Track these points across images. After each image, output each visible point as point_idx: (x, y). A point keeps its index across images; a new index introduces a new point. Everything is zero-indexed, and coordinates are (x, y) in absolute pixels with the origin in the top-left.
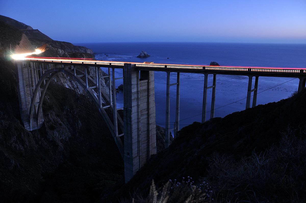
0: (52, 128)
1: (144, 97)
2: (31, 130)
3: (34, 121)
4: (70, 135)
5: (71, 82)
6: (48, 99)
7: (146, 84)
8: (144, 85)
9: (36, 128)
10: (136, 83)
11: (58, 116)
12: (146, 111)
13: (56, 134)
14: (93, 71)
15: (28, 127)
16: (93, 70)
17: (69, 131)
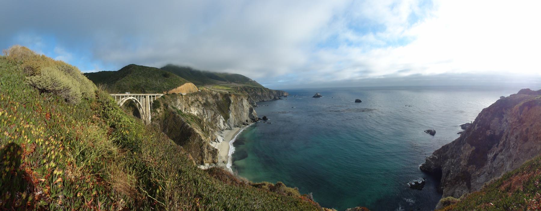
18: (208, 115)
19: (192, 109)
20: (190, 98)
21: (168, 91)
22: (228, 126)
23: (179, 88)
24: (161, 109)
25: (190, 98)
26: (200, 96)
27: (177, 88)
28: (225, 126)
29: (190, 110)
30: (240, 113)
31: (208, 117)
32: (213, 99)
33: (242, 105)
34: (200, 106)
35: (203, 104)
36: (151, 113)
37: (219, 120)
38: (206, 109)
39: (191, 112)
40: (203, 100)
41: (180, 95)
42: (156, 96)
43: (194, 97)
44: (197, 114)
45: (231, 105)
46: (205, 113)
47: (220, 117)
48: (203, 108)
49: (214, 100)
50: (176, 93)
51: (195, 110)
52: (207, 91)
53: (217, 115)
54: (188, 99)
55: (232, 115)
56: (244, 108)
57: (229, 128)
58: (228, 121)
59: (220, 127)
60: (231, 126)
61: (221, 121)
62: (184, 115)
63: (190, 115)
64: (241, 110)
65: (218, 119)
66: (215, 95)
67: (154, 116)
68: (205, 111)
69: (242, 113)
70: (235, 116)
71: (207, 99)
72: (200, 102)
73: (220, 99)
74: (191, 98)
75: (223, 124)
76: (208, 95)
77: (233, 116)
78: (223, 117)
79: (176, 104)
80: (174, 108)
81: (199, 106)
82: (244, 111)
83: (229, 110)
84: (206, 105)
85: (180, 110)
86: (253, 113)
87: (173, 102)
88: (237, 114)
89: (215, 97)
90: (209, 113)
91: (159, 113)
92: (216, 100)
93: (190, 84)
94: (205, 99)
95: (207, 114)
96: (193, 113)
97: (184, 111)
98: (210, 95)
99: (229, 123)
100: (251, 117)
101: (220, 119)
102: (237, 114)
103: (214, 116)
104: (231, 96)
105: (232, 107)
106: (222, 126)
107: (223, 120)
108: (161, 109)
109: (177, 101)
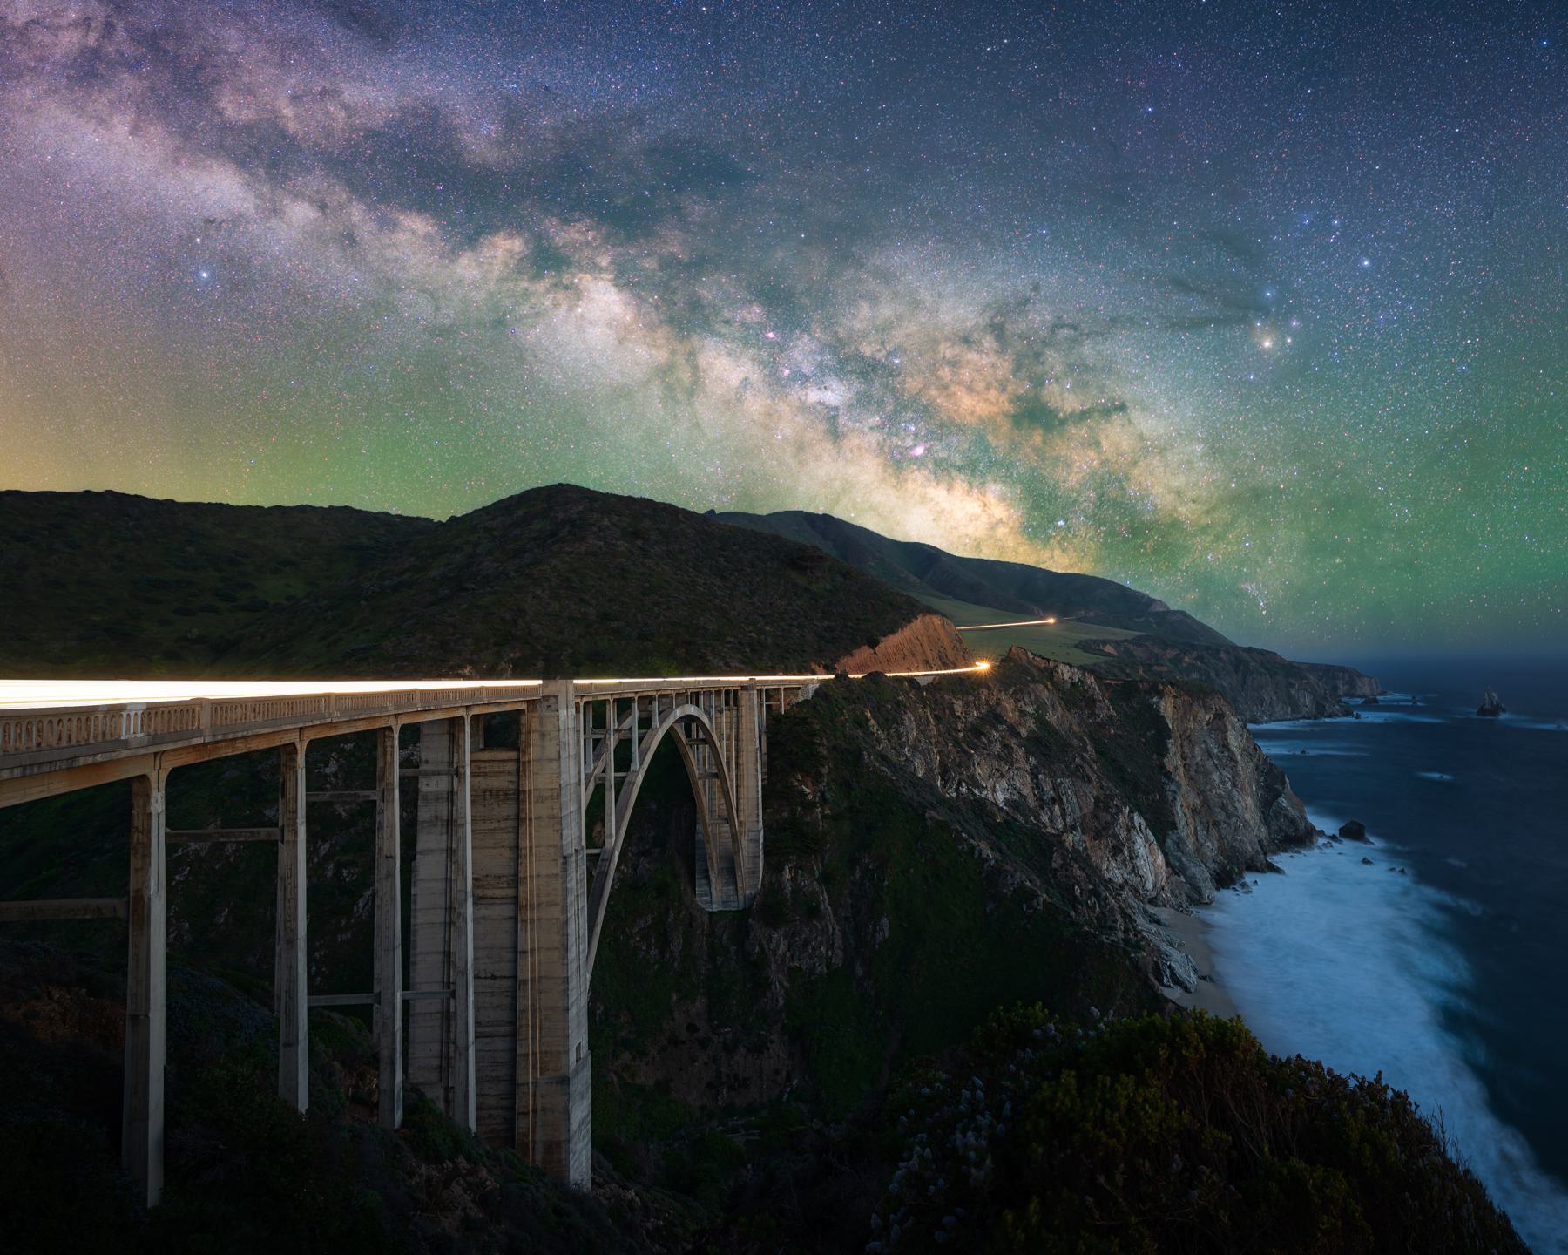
1: (499, 821)
5: (1034, 776)
6: (824, 817)
7: (511, 766)
8: (496, 769)
12: (505, 886)
14: (1201, 749)
24: (817, 778)
25: (958, 706)
26: (1006, 691)
30: (1220, 796)
32: (1069, 711)
33: (1225, 746)
34: (1020, 752)
35: (1028, 738)
36: (764, 809)
37: (1129, 839)
39: (976, 791)
43: (979, 699)
44: (1007, 802)
47: (1132, 819)
48: (1033, 761)
52: (1029, 662)
55: (1182, 806)
58: (1169, 842)
60: (1193, 877)
64: (1223, 782)
65: (1123, 834)
68: (1048, 787)
69: (1229, 793)
70: (1194, 811)
71: (1041, 706)
72: (1014, 732)
73: (1105, 709)
74: (967, 705)
76: (1041, 687)
77: (1186, 811)
78: (1143, 822)
82: (1239, 783)
83: (1168, 775)
88: (1205, 802)
89: (1074, 697)
90: (1069, 794)
93: (937, 620)
97: (939, 783)
99: (1180, 861)
101: (1133, 833)
102: (1205, 802)
103: (1095, 817)
104: (1161, 694)
105: (1173, 761)
109: (902, 719)
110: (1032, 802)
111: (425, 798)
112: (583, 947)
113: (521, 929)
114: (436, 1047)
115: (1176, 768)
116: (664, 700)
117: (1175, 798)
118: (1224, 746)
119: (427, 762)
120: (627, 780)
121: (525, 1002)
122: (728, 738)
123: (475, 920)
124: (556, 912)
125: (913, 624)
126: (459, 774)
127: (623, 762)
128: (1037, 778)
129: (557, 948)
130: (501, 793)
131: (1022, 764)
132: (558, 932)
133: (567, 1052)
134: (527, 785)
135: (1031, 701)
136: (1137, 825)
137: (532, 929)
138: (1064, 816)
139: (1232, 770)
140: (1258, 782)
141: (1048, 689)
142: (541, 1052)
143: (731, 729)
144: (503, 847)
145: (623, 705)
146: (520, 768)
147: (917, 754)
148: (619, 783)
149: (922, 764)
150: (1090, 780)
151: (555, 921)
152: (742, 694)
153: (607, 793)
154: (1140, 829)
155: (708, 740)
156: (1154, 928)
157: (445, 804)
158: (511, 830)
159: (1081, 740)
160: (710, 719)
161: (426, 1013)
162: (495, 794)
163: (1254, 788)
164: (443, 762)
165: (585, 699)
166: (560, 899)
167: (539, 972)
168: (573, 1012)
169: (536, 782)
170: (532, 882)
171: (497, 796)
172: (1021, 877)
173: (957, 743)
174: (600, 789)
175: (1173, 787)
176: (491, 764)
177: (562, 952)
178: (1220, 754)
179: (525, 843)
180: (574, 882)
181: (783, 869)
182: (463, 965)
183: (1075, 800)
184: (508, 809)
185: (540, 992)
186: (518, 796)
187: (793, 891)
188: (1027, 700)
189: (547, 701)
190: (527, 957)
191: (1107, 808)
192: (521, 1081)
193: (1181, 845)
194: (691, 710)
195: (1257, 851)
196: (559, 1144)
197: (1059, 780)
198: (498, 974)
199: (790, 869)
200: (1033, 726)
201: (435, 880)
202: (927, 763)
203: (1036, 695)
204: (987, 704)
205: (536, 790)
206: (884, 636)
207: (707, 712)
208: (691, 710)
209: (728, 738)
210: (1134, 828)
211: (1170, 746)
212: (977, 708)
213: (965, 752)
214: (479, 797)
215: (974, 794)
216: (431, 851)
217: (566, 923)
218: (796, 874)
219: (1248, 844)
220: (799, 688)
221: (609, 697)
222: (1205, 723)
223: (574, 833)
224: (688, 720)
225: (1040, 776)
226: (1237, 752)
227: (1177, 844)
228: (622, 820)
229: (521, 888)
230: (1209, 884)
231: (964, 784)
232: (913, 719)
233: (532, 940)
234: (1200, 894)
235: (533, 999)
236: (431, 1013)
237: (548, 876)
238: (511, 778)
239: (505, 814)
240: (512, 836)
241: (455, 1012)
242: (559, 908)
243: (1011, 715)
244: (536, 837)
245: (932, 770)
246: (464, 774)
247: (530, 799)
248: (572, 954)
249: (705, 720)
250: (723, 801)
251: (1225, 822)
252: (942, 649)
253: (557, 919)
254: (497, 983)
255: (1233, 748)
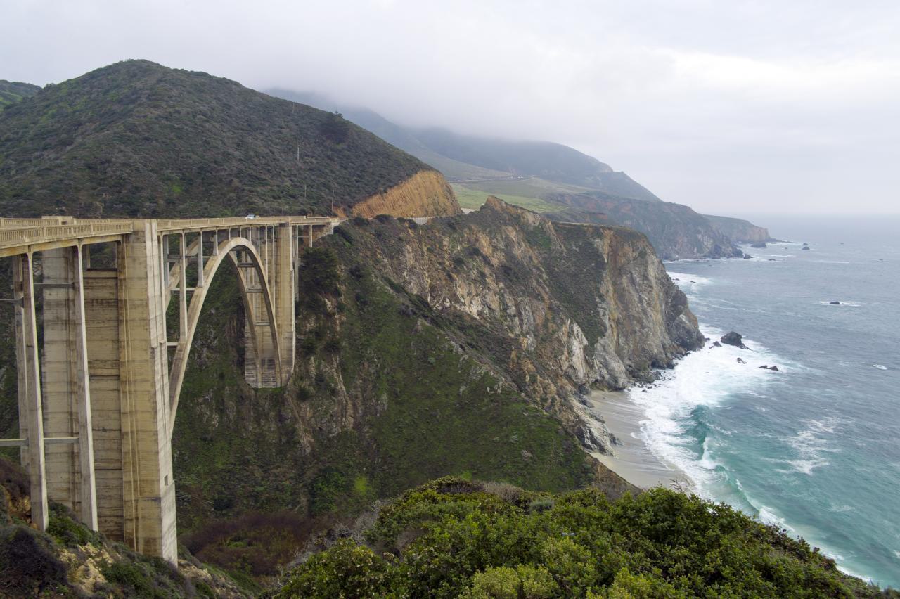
0: (303, 396)
1: (104, 322)
2: (260, 386)
3: (269, 365)
4: (351, 425)
6: (342, 323)
8: (100, 284)
9: (272, 385)
10: (63, 275)
11: (343, 369)
12: (110, 367)
13: (307, 410)
15: (253, 377)
16: (629, 275)
17: (353, 415)
18: (521, 320)
19: (460, 292)
20: (448, 239)
21: (350, 207)
22: (604, 372)
23: (395, 193)
27: (385, 192)
28: (592, 367)
29: (455, 295)
31: (525, 327)
32: (531, 248)
33: (645, 277)
35: (498, 269)
36: (296, 315)
37: (568, 342)
38: (512, 293)
39: (458, 306)
40: (495, 248)
41: (407, 225)
42: (314, 226)
44: (480, 314)
45: (606, 274)
46: (512, 310)
47: (571, 328)
48: (501, 285)
49: (533, 253)
50: (395, 214)
51: (469, 294)
53: (559, 321)
54: (441, 243)
55: (609, 319)
56: (654, 293)
57: (607, 377)
58: (598, 346)
59: (570, 371)
61: (577, 347)
62: (437, 321)
63: (461, 323)
65: (564, 339)
66: (536, 228)
67: (311, 332)
69: (644, 311)
70: (618, 322)
71: (509, 244)
72: (486, 261)
73: (559, 246)
74: (453, 240)
75: (586, 360)
76: (510, 228)
77: (612, 324)
78: (579, 330)
79: (398, 269)
80: (399, 289)
81: (483, 275)
84: (511, 273)
85: (417, 296)
86: (683, 317)
87: (386, 260)
89: (534, 236)
91: (334, 314)
92: (540, 254)
93: (432, 176)
94: (501, 246)
95: (519, 314)
96: (467, 309)
97: (429, 300)
98: (517, 231)
99: (605, 359)
100: (675, 332)
103: (545, 326)
105: (607, 287)
106: (582, 370)
107: (581, 343)
108: (337, 293)
109: (403, 253)
110: (498, 314)
111: (49, 304)
112: (167, 410)
113: (123, 397)
114: (65, 476)
115: (608, 291)
116: (222, 234)
117: (604, 315)
118: (644, 276)
119: (49, 278)
120: (195, 294)
121: (127, 447)
122: (270, 263)
123: (91, 391)
124: (147, 386)
125: (413, 178)
126: (74, 287)
127: (193, 281)
128: (503, 296)
129: (149, 411)
130: (104, 302)
131: (492, 285)
132: (149, 400)
133: (158, 481)
134: (124, 296)
135: (502, 239)
136: (575, 332)
137: (130, 398)
138: (521, 325)
139: (648, 293)
140: (667, 303)
141: (515, 228)
142: (140, 480)
143: (272, 256)
144: (107, 340)
145: (192, 237)
146: (118, 283)
147: (414, 277)
148: (190, 295)
149: (416, 284)
150: (543, 300)
151: (147, 393)
152: (280, 230)
153: (181, 303)
154: (577, 334)
155: (255, 264)
156: (581, 406)
157: (64, 308)
158: (113, 328)
159: (538, 269)
160: (256, 248)
161: (57, 453)
162: (102, 302)
163: (664, 307)
164: (60, 278)
165: (164, 233)
166: (150, 378)
167: (137, 427)
168: (161, 455)
169: (130, 294)
170: (128, 365)
171: (102, 303)
172: (484, 367)
173: (444, 270)
174: (175, 296)
175: (604, 306)
176: (96, 280)
177: (153, 413)
178: (641, 282)
179: (123, 337)
180: (160, 366)
181: (309, 359)
182: (84, 421)
183: (531, 314)
184: (111, 314)
185: (138, 441)
186: (117, 304)
187: (316, 376)
188: (499, 238)
189: (137, 234)
190: (127, 417)
191: (554, 320)
192: (126, 499)
193: (606, 348)
194: (242, 241)
195: (661, 352)
196: (155, 540)
197: (520, 299)
198: (106, 428)
199: (315, 359)
200: (503, 258)
201: (59, 362)
202: (420, 284)
203: (506, 234)
204: (469, 241)
205: (129, 300)
206: (391, 187)
207: (254, 243)
208: (242, 241)
209: (270, 263)
210: (573, 334)
211: (604, 275)
212: (461, 243)
213: (450, 276)
214: (89, 303)
215: (455, 308)
216: (53, 342)
217: (155, 394)
218: (320, 363)
219: (654, 347)
220: (324, 226)
221: (181, 232)
222: (631, 259)
223: (158, 332)
224: (240, 250)
225: (505, 295)
226: (653, 281)
227: (604, 347)
228: (193, 321)
229: (122, 369)
230: (624, 376)
231: (448, 300)
232: (411, 250)
233: (131, 405)
234: (616, 381)
235: (133, 445)
236: (60, 453)
237: (141, 361)
238: (111, 291)
239: (107, 317)
240: (113, 333)
241: (78, 453)
242: (149, 384)
243: (486, 249)
244: (131, 333)
245: (424, 289)
246: (79, 288)
247: (126, 306)
248: (160, 415)
249: (253, 249)
250: (265, 309)
251: (640, 331)
252: (436, 198)
253: (149, 391)
254: (107, 434)
255: (650, 278)
